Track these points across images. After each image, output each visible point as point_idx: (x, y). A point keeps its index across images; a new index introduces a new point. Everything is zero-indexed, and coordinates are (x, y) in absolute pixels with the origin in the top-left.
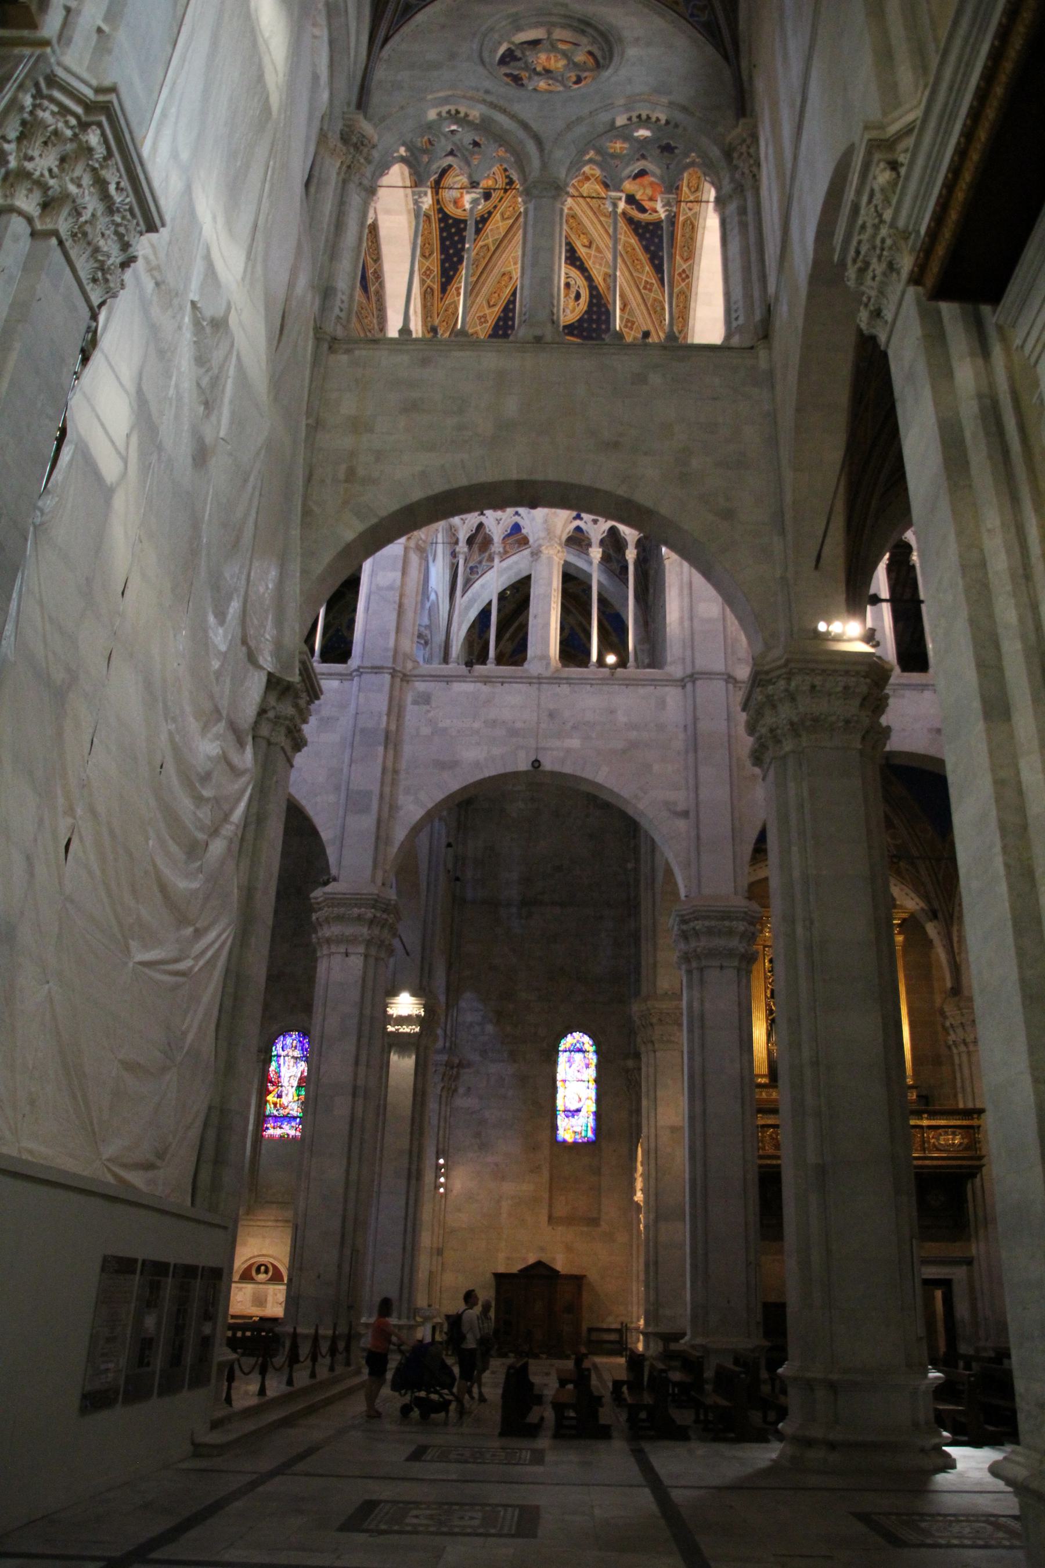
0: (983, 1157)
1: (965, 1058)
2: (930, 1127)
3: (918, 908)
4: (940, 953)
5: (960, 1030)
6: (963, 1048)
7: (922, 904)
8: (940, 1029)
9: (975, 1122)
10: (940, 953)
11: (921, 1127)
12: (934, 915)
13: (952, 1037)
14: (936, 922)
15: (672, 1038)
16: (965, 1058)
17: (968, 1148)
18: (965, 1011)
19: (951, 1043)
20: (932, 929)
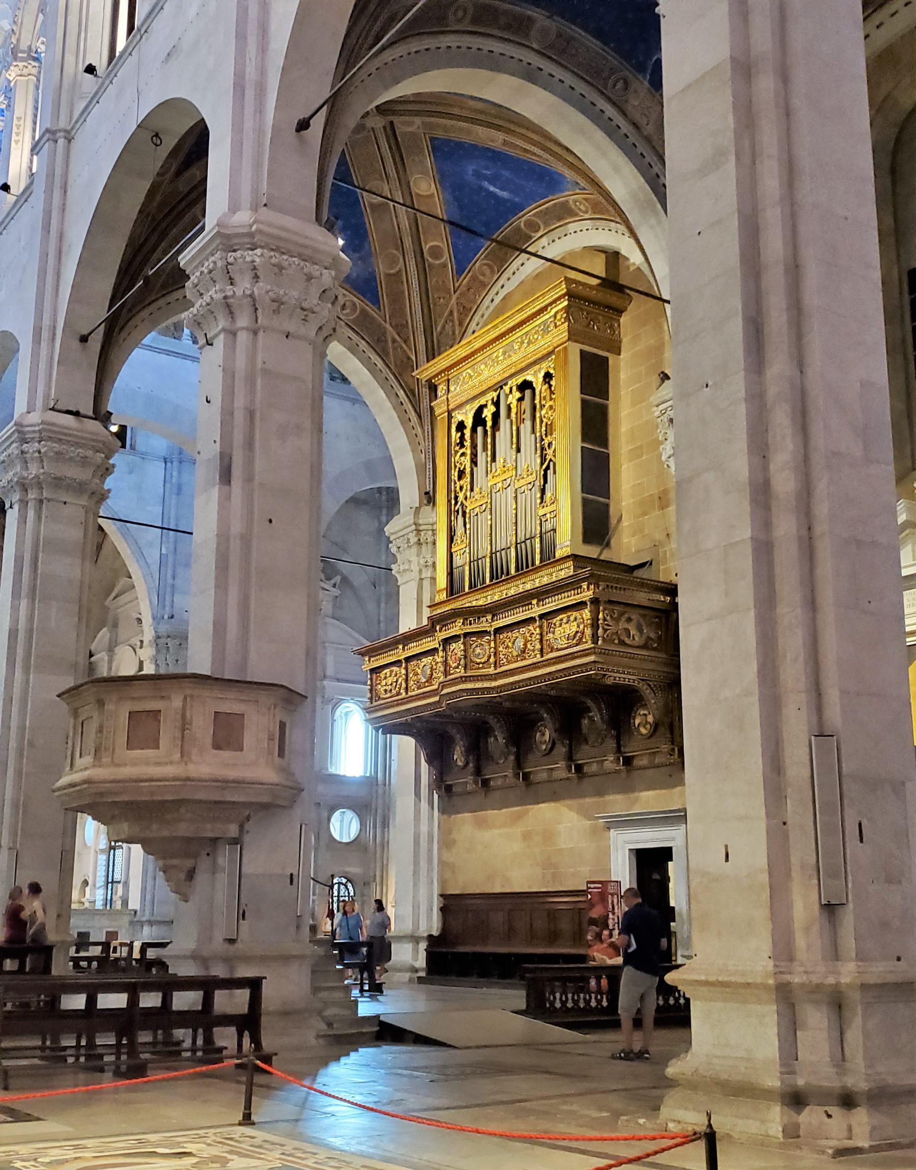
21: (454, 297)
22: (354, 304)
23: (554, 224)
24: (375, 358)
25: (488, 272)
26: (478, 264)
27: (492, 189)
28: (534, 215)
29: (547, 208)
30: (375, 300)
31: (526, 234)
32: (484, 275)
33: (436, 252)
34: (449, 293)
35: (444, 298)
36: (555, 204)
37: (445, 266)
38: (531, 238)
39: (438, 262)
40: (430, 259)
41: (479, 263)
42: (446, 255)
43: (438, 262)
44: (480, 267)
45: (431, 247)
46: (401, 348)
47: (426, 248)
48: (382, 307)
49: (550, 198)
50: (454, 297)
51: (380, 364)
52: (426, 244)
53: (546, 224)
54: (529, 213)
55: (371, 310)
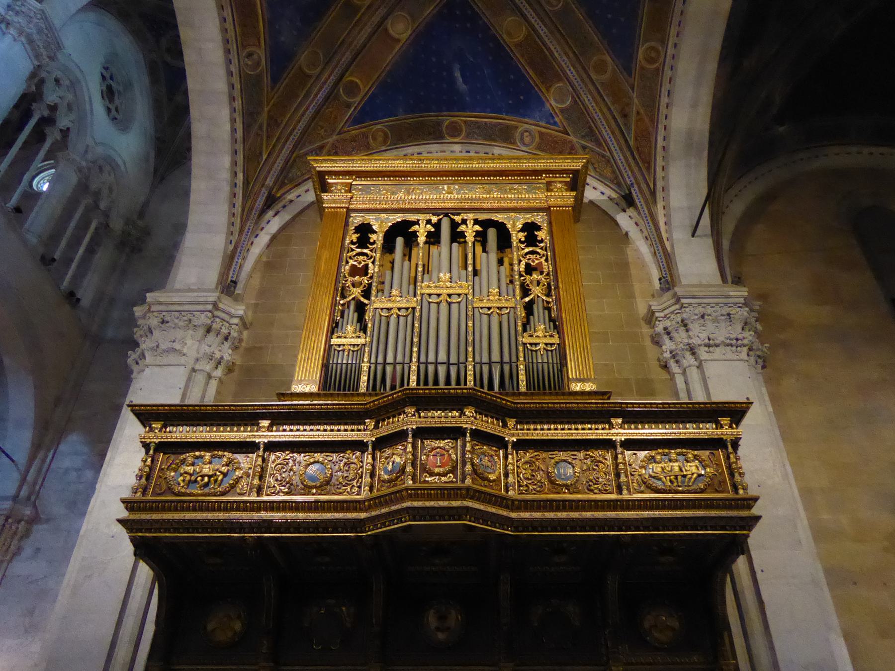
0: (756, 499)
1: (694, 374)
2: (631, 444)
3: (604, 198)
4: (641, 247)
5: (681, 336)
6: (688, 360)
7: (608, 192)
8: (648, 342)
9: (726, 432)
10: (641, 247)
11: (608, 444)
12: (628, 201)
13: (668, 345)
14: (631, 209)
15: (177, 346)
16: (694, 374)
17: (715, 484)
18: (683, 301)
19: (667, 355)
20: (625, 220)
21: (335, 137)
22: (258, 64)
23: (476, 139)
24: (239, 126)
25: (380, 139)
26: (379, 127)
27: (457, 74)
28: (465, 122)
29: (486, 123)
30: (275, 80)
31: (441, 132)
32: (374, 139)
33: (352, 89)
34: (333, 131)
35: (326, 131)
36: (500, 124)
37: (349, 106)
38: (442, 137)
39: (345, 98)
40: (341, 91)
41: (379, 127)
42: (358, 99)
43: (345, 98)
44: (378, 130)
45: (352, 82)
46: (262, 139)
47: (348, 78)
48: (275, 90)
49: (504, 116)
50: (335, 137)
51: (239, 134)
52: (350, 75)
53: (468, 136)
54: (461, 118)
55: (266, 80)
